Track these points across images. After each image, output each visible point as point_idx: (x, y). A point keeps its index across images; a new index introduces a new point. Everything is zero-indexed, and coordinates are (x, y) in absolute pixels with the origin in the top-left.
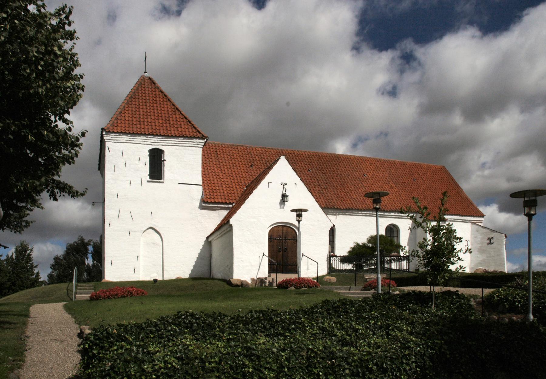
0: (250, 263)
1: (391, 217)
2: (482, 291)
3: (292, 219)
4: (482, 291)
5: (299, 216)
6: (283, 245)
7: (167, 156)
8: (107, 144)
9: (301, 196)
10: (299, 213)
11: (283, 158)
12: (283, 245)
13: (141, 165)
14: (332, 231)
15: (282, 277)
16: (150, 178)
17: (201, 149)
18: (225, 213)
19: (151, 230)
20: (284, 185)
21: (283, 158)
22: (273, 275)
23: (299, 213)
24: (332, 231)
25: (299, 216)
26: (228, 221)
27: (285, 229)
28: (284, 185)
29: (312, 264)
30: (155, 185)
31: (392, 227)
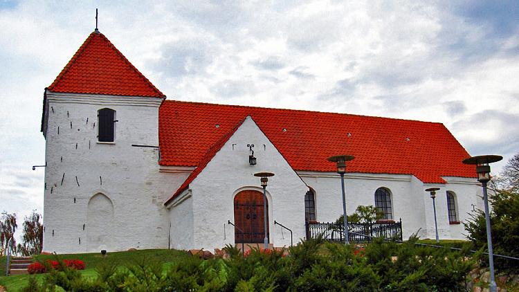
0: (212, 231)
1: (381, 179)
2: (437, 237)
3: (256, 183)
4: (437, 237)
5: (264, 180)
6: (251, 211)
7: (117, 117)
8: (51, 105)
9: (271, 158)
10: (264, 176)
11: (249, 118)
12: (251, 211)
13: (90, 127)
14: (310, 196)
15: (247, 248)
16: (99, 140)
17: (158, 109)
18: (184, 177)
19: (100, 196)
20: (251, 147)
21: (249, 118)
22: (240, 246)
23: (264, 176)
24: (310, 196)
25: (264, 180)
26: (187, 187)
27: (254, 194)
28: (251, 147)
29: (286, 230)
30: (105, 149)
31: (243, 201)
